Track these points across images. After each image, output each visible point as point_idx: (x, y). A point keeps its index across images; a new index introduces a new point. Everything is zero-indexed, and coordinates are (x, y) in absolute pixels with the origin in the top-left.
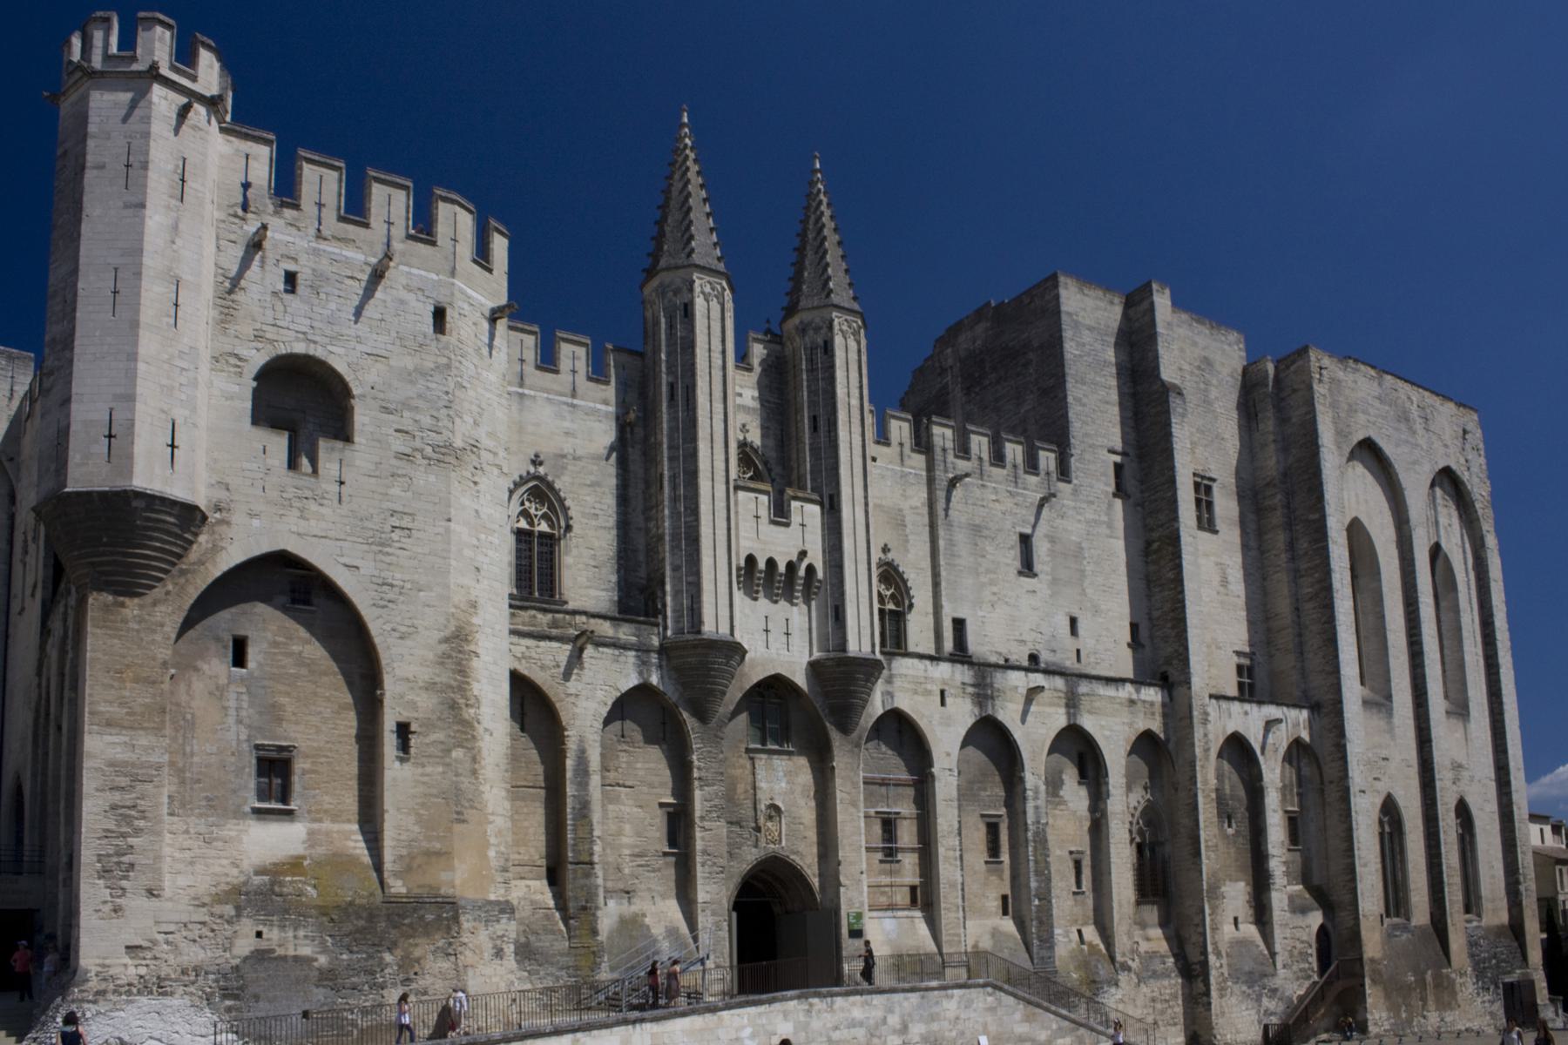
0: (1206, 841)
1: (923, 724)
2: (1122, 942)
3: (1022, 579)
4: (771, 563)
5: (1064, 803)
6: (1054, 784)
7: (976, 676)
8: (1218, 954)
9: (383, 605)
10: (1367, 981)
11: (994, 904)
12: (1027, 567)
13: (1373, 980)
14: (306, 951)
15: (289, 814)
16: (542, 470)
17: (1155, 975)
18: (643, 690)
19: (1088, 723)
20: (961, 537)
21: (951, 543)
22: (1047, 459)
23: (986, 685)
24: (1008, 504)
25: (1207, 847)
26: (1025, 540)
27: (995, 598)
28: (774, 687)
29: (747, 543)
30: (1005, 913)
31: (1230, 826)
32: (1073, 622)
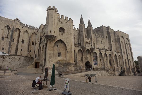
1: (96, 52)
2: (109, 68)
6: (104, 57)
12: (102, 43)
14: (62, 66)
15: (60, 57)
18: (80, 50)
19: (106, 53)
22: (103, 37)
28: (88, 50)
29: (86, 41)
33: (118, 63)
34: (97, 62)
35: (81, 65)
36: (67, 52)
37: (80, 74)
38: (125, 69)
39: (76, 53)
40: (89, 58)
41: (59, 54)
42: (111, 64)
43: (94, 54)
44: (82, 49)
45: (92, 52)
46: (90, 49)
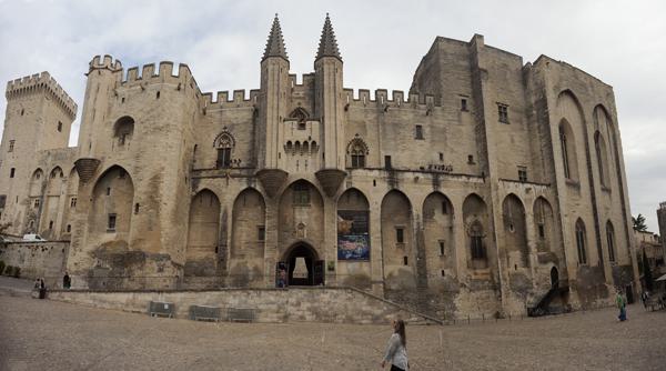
4: (298, 143)
8: (505, 280)
9: (136, 172)
11: (400, 259)
12: (419, 136)
15: (114, 231)
17: (478, 289)
18: (250, 190)
19: (443, 190)
21: (384, 130)
24: (411, 116)
28: (302, 185)
32: (441, 155)
33: (532, 244)
34: (369, 242)
35: (251, 268)
36: (134, 208)
37: (123, 297)
38: (572, 275)
39: (222, 209)
40: (315, 226)
41: (112, 218)
42: (479, 251)
43: (353, 199)
44: (263, 184)
45: (325, 190)
46: (316, 174)
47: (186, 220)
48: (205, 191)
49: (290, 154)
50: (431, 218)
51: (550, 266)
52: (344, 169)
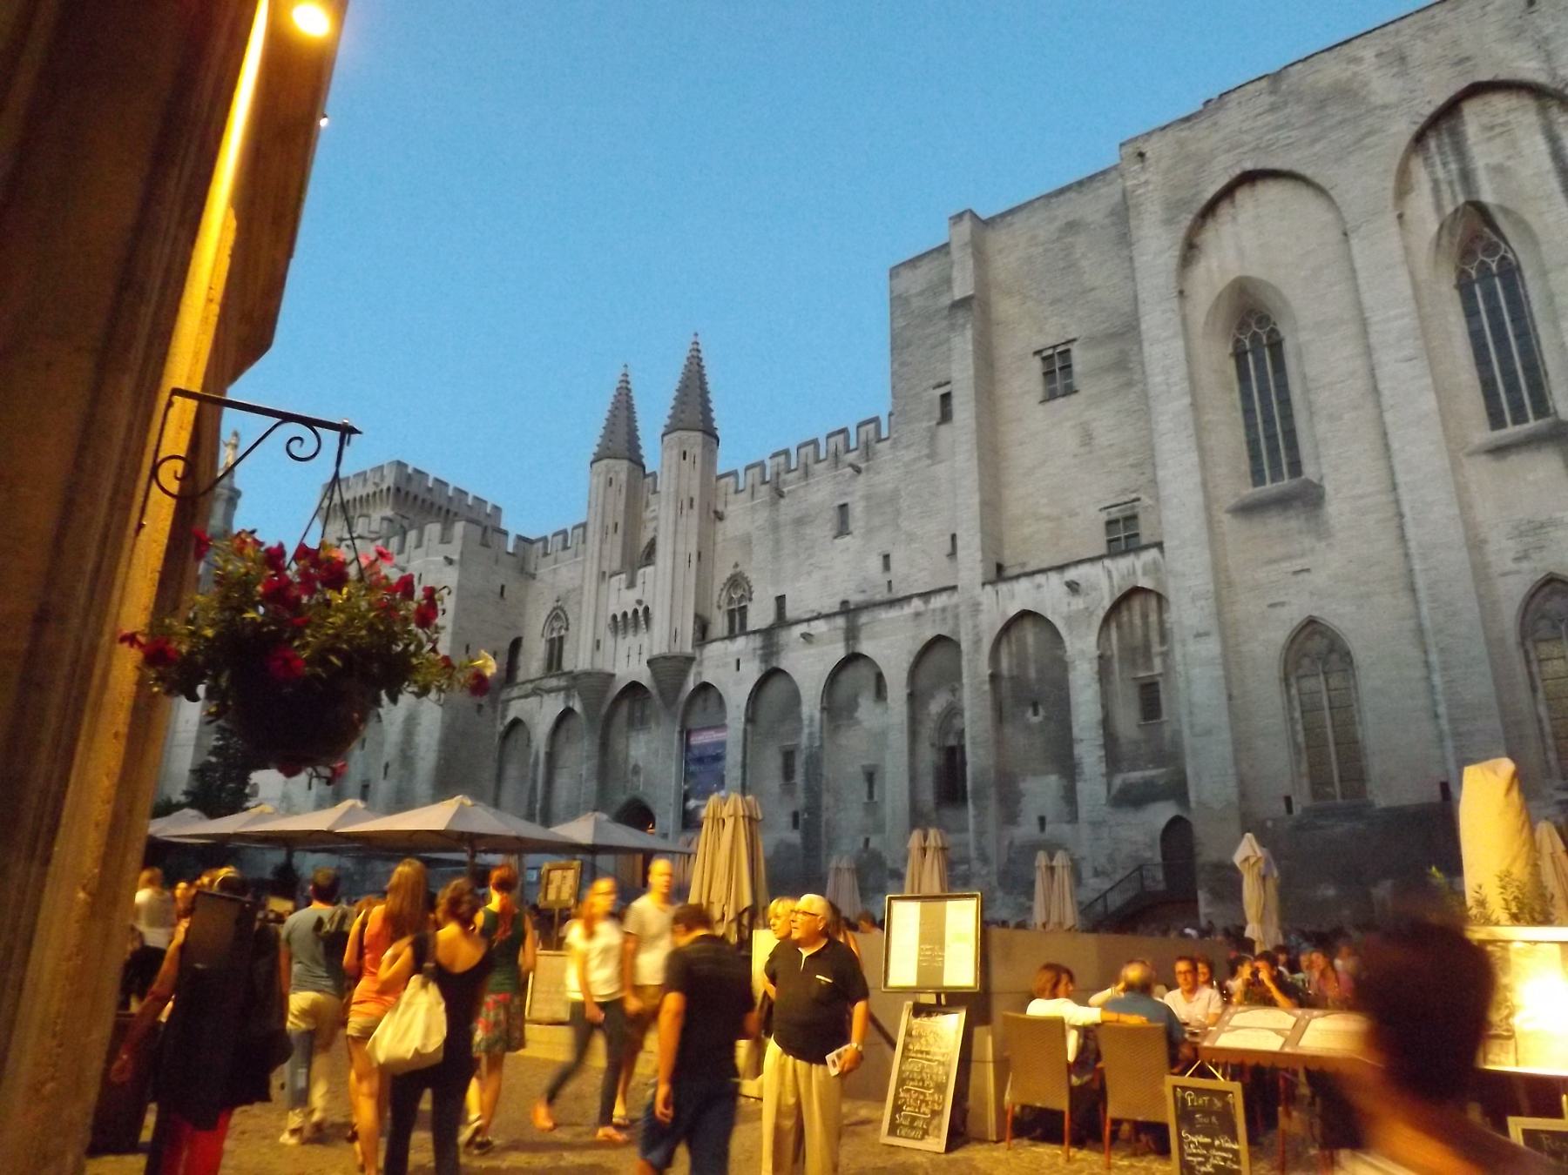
0: (973, 738)
3: (837, 541)
4: (625, 614)
5: (858, 722)
7: (764, 641)
8: (985, 860)
10: (1202, 896)
11: (785, 819)
13: (1212, 891)
16: (560, 603)
18: (567, 713)
19: (865, 648)
20: (786, 533)
21: (777, 542)
23: (772, 645)
25: (973, 743)
26: (843, 507)
27: (812, 568)
28: (634, 688)
30: (795, 824)
31: (1036, 713)
32: (886, 557)
33: (1089, 753)
36: (382, 770)
45: (662, 693)
47: (488, 774)
48: (517, 722)
49: (620, 637)
50: (851, 717)
51: (1163, 814)
52: (688, 649)
